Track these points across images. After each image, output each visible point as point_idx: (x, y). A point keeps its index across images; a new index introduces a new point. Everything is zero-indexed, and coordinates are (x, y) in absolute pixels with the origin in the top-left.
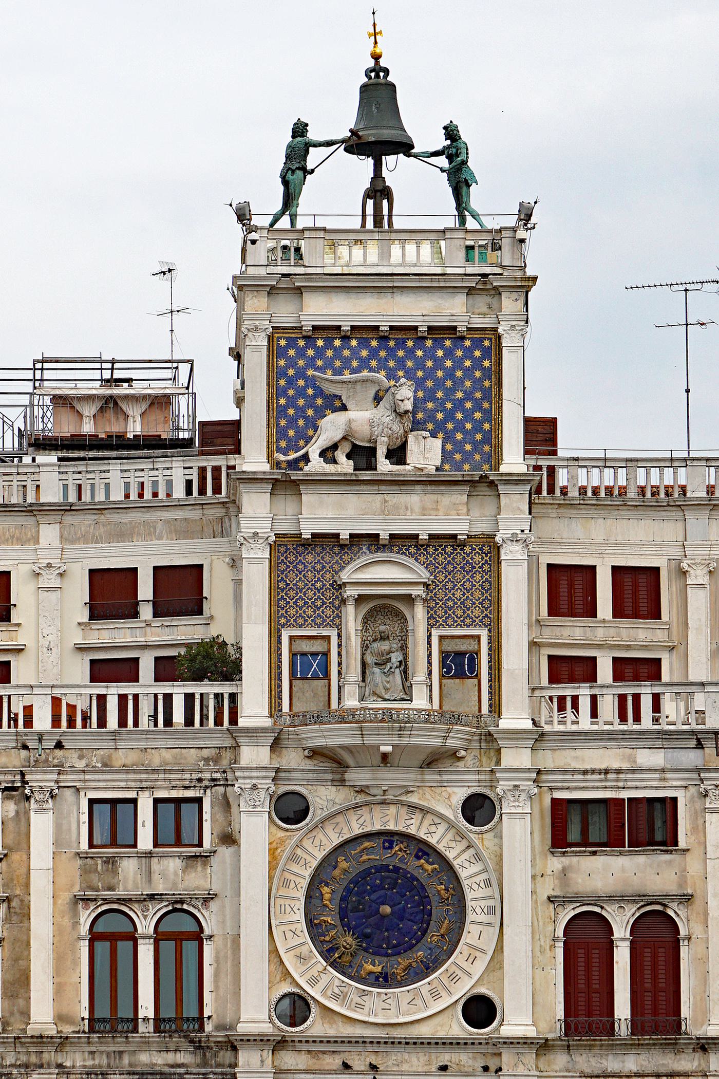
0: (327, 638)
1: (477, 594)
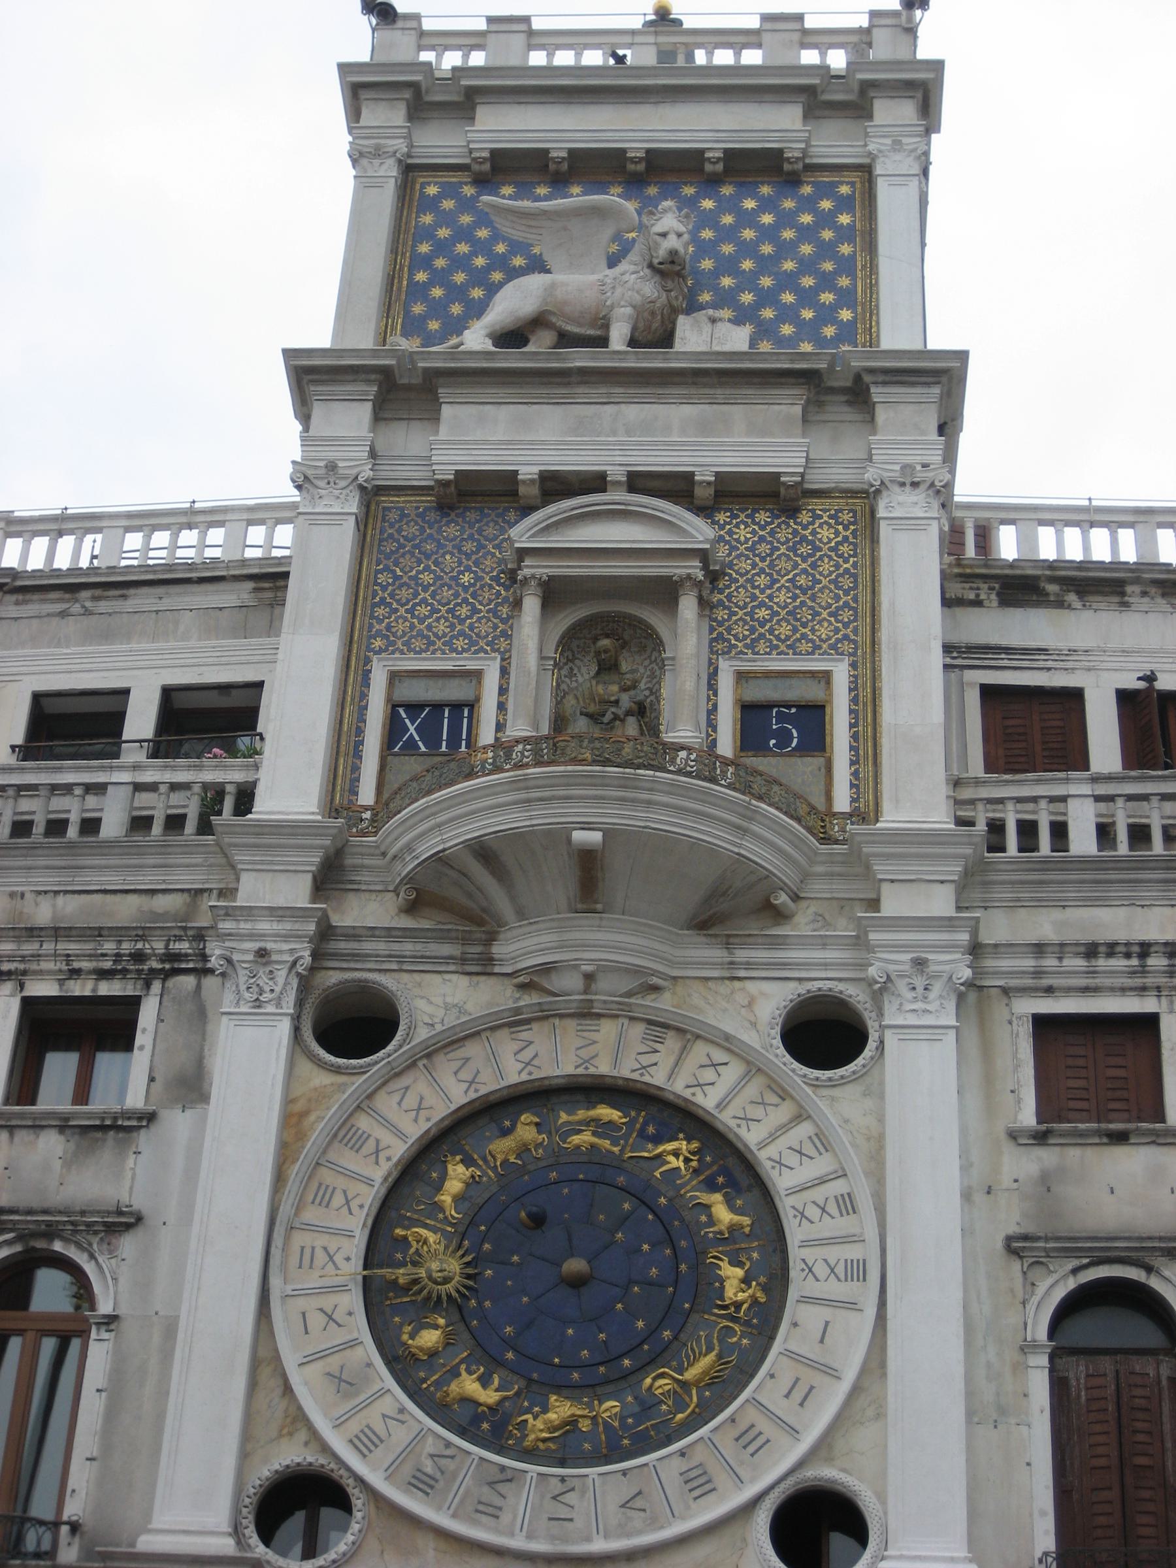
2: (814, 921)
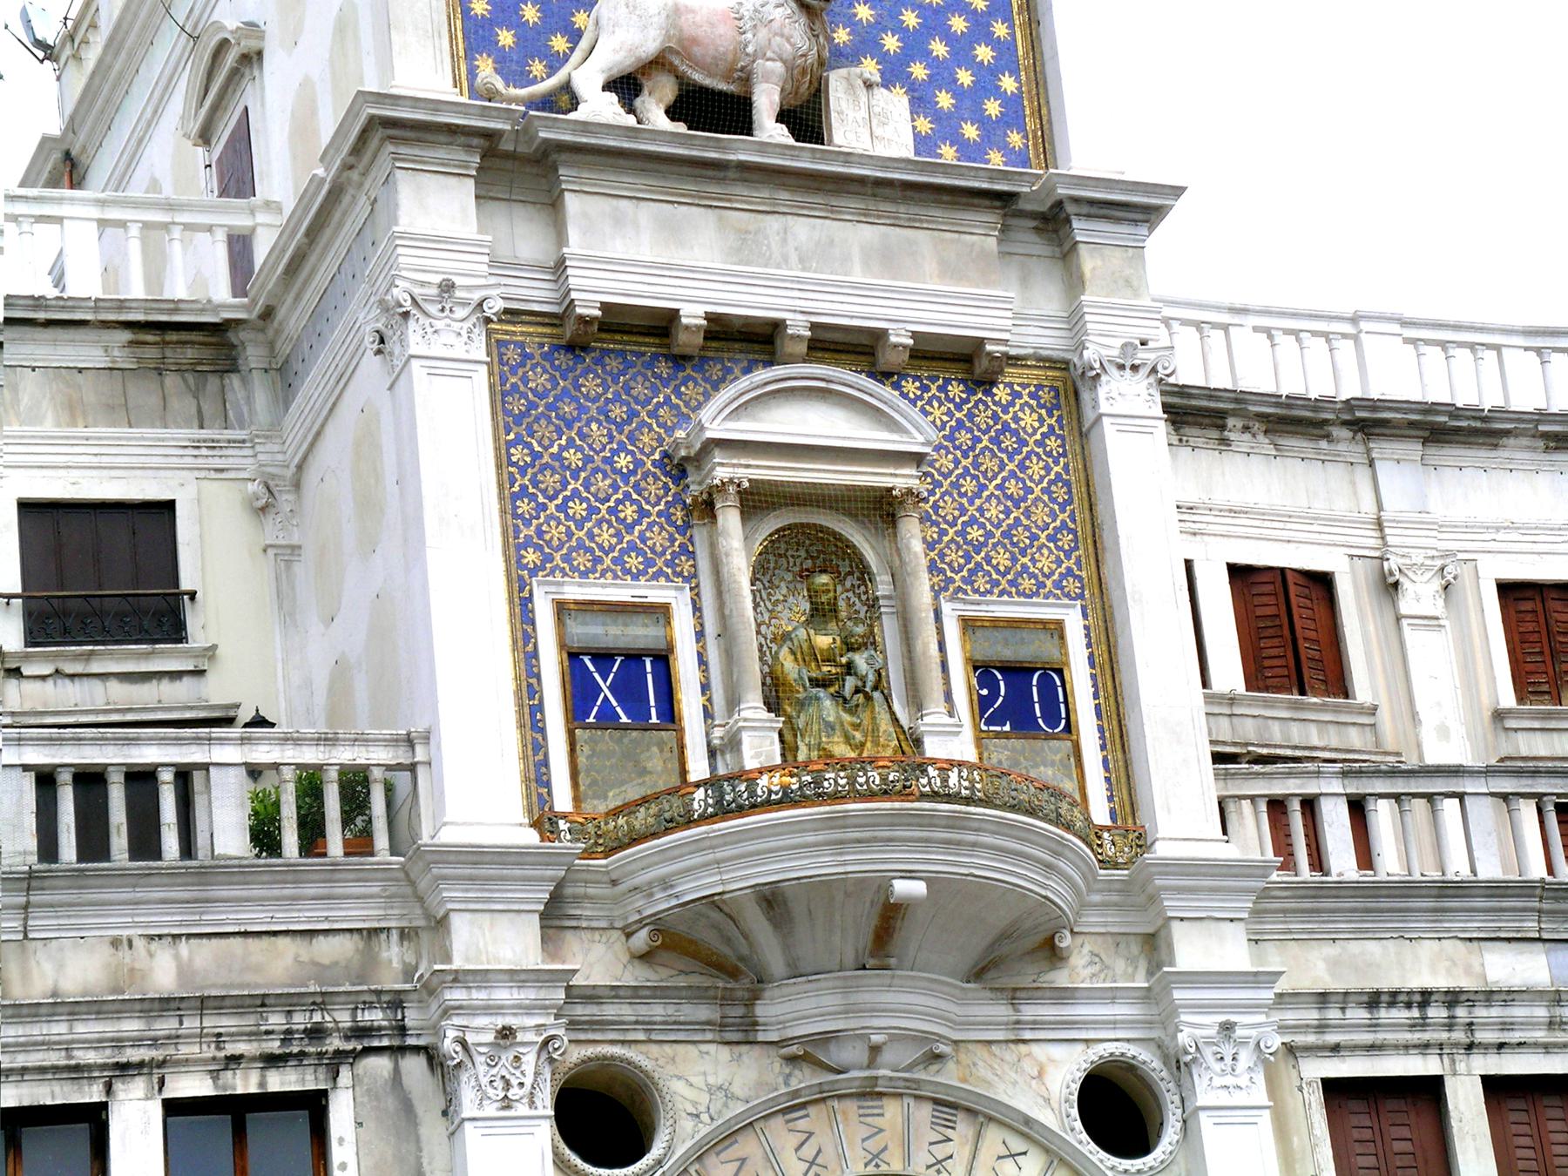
0: (661, 612)
1: (1041, 515)
2: (1092, 963)
